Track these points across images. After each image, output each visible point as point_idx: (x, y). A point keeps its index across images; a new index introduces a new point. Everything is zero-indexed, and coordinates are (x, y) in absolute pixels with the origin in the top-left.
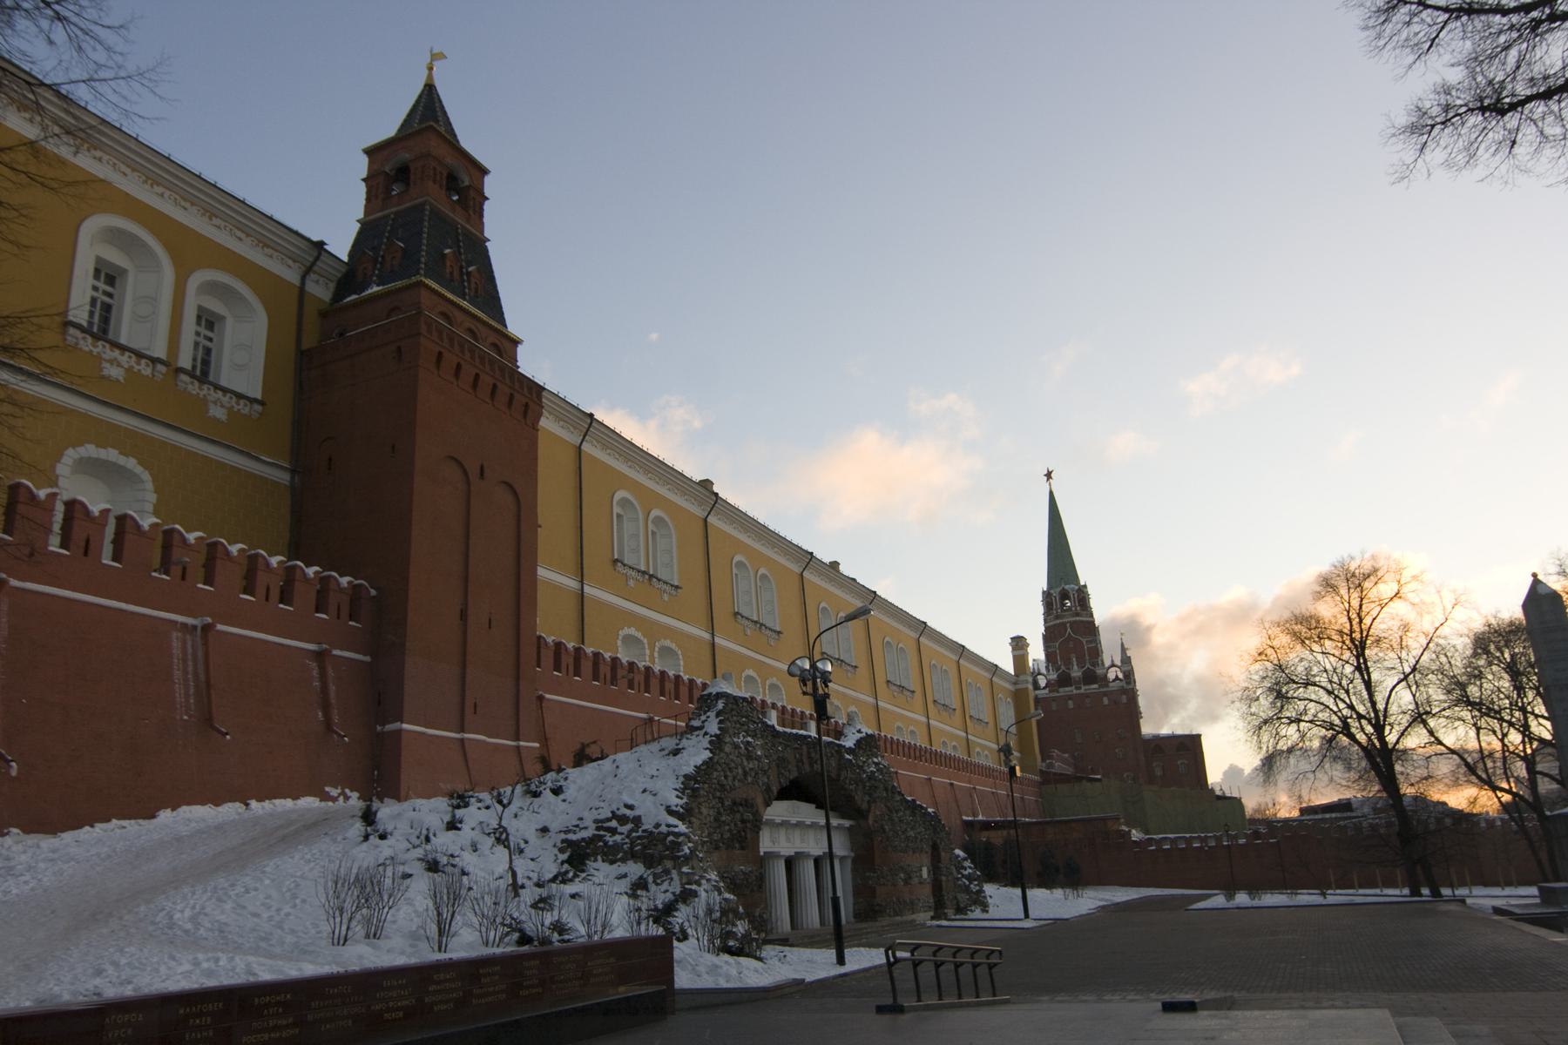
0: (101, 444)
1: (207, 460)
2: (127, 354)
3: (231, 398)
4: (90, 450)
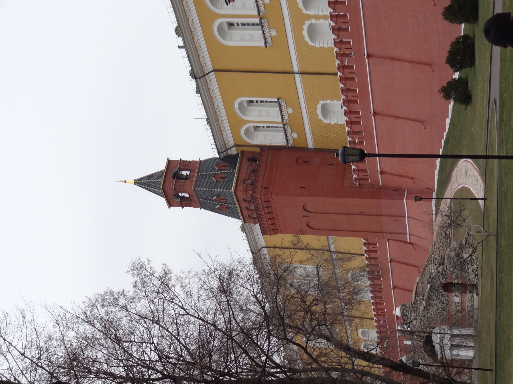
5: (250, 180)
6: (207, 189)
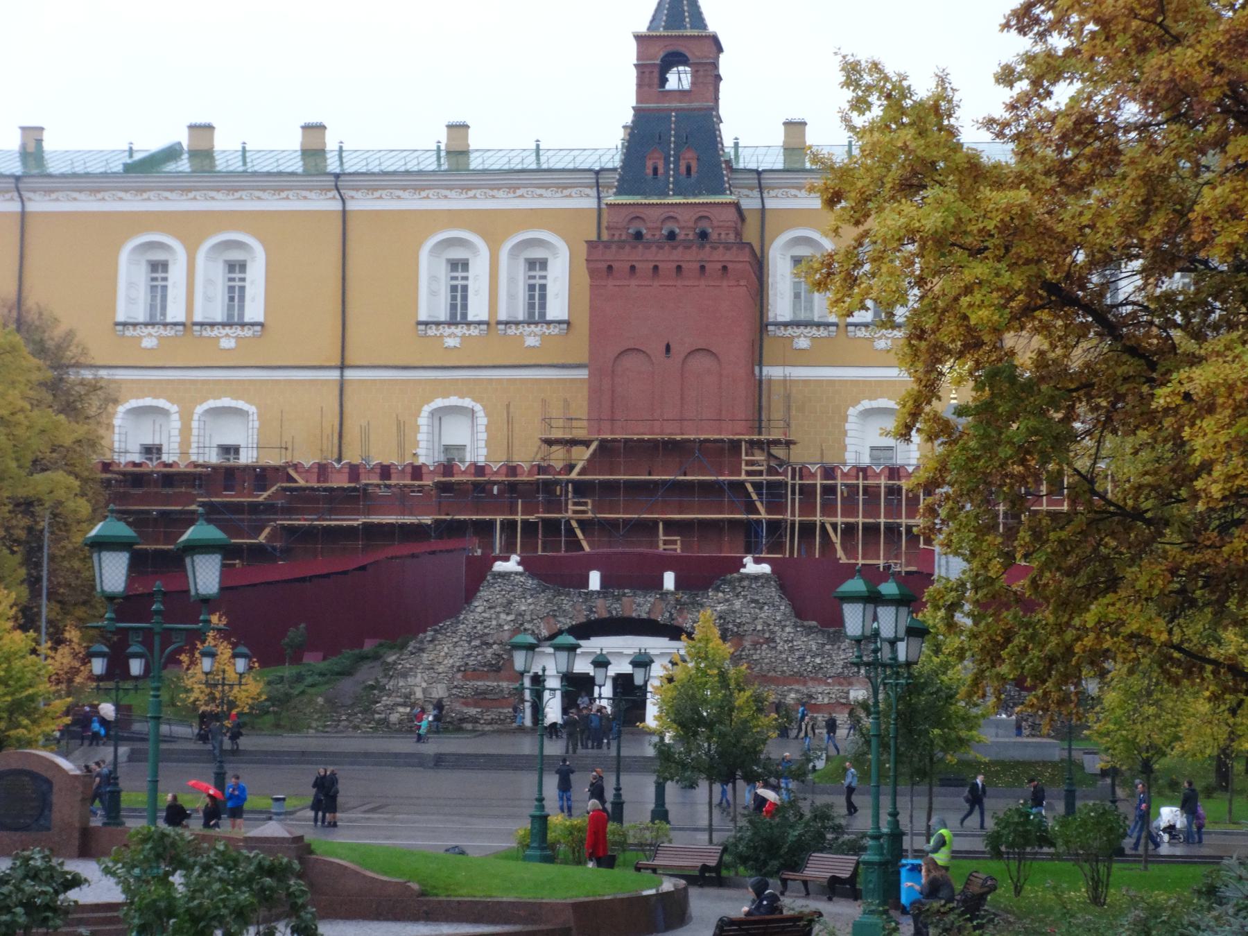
0: (446, 395)
1: (524, 381)
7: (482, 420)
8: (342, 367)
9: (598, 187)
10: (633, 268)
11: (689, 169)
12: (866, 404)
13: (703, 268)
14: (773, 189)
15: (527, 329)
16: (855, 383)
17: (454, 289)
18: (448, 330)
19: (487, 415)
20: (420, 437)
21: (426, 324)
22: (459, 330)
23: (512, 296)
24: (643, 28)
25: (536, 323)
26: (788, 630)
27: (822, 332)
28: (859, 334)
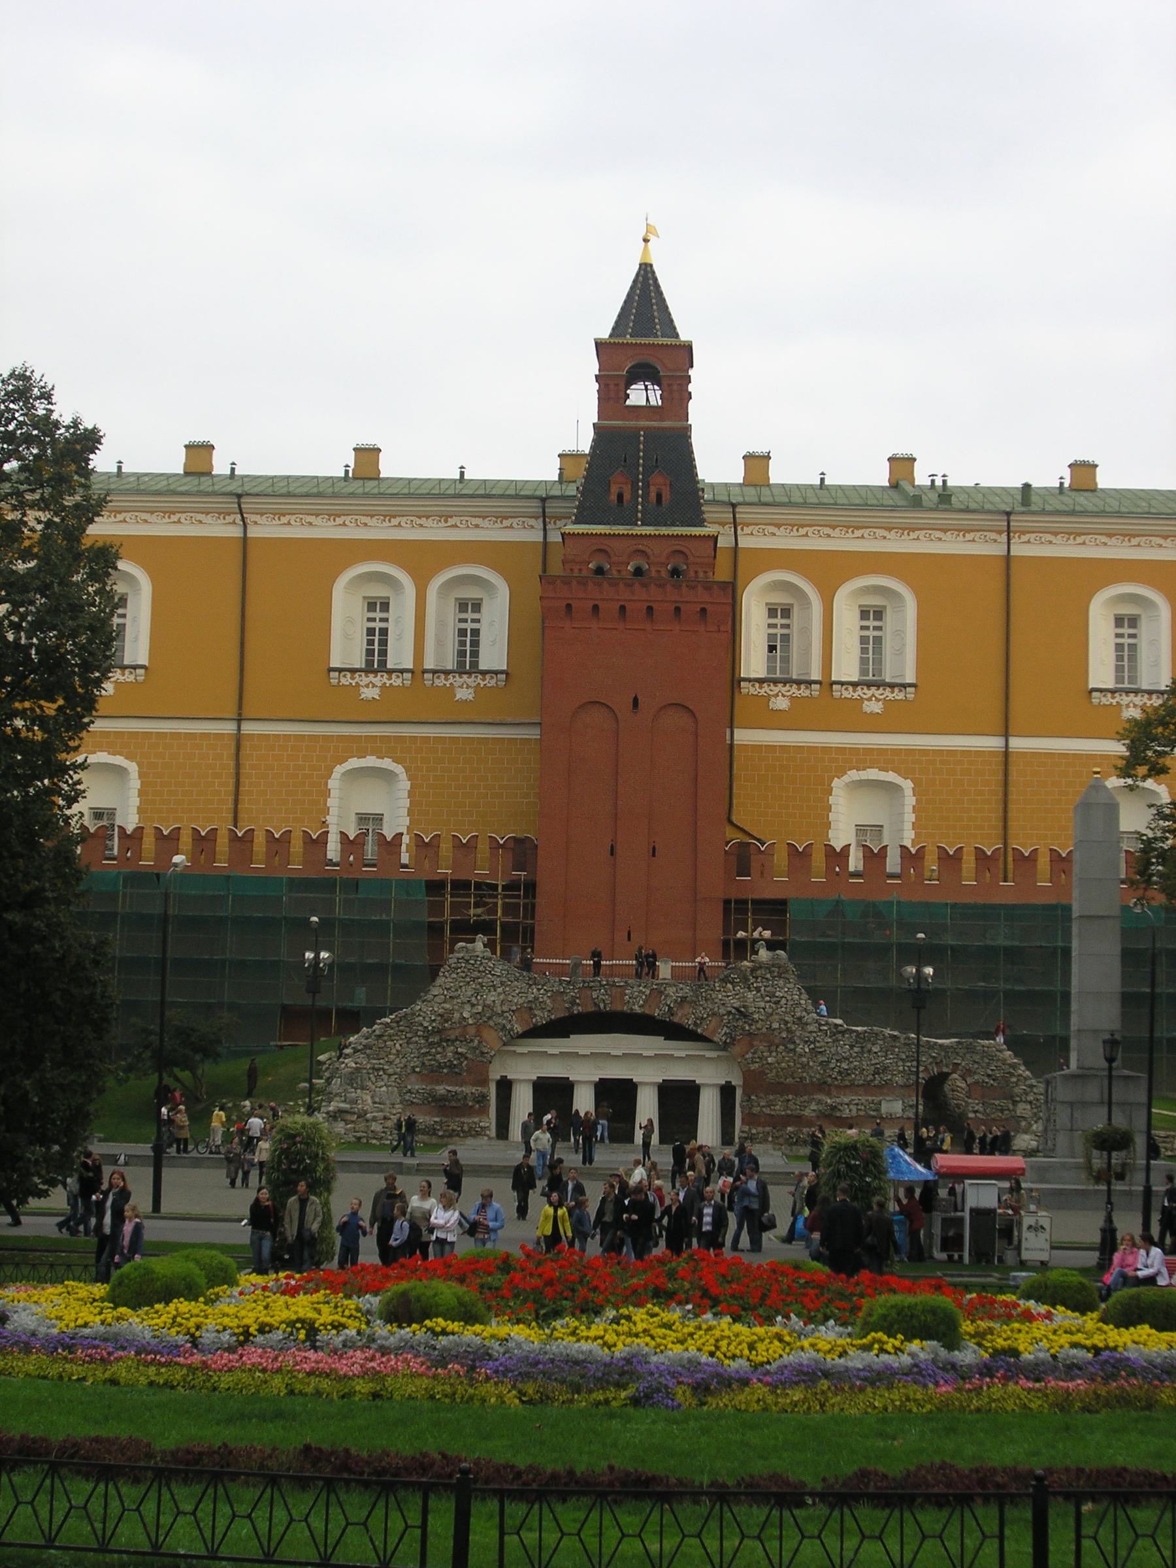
2: (379, 674)
3: (476, 677)
4: (354, 763)
5: (685, 567)
6: (641, 454)
7: (404, 784)
8: (239, 721)
9: (544, 517)
10: (596, 608)
11: (659, 497)
12: (853, 775)
13: (678, 610)
14: (748, 525)
15: (458, 680)
16: (841, 750)
17: (371, 632)
18: (364, 680)
19: (410, 778)
20: (330, 802)
21: (340, 670)
22: (379, 680)
23: (440, 643)
24: (605, 334)
25: (469, 673)
26: (810, 1028)
27: (804, 692)
28: (846, 694)
